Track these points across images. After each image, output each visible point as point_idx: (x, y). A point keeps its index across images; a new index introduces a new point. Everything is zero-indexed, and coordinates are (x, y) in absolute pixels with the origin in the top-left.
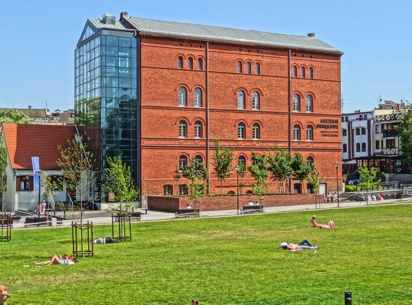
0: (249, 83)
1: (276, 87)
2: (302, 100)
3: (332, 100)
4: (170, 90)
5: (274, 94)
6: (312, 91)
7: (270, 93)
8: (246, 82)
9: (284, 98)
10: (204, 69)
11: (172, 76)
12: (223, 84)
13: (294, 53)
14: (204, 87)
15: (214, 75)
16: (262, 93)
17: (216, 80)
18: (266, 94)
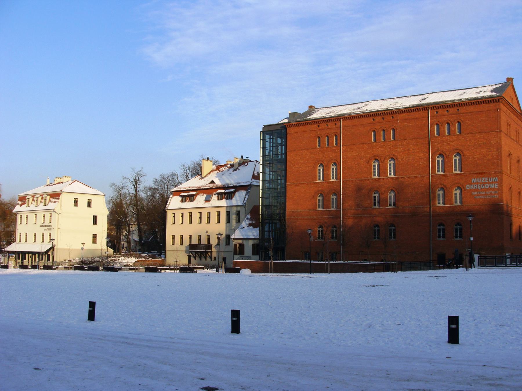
0: (383, 151)
1: (414, 150)
2: (446, 160)
3: (488, 155)
4: (309, 168)
5: (412, 158)
6: (461, 148)
7: (407, 158)
8: (380, 150)
9: (424, 161)
10: (339, 145)
11: (311, 156)
12: (356, 155)
13: (436, 110)
14: (339, 160)
15: (347, 148)
16: (397, 160)
17: (349, 153)
18: (402, 160)
